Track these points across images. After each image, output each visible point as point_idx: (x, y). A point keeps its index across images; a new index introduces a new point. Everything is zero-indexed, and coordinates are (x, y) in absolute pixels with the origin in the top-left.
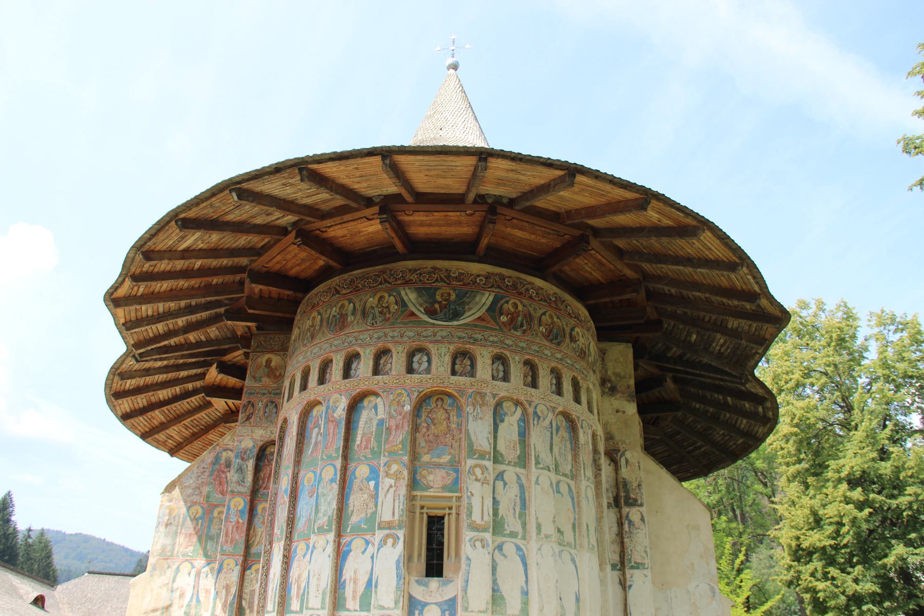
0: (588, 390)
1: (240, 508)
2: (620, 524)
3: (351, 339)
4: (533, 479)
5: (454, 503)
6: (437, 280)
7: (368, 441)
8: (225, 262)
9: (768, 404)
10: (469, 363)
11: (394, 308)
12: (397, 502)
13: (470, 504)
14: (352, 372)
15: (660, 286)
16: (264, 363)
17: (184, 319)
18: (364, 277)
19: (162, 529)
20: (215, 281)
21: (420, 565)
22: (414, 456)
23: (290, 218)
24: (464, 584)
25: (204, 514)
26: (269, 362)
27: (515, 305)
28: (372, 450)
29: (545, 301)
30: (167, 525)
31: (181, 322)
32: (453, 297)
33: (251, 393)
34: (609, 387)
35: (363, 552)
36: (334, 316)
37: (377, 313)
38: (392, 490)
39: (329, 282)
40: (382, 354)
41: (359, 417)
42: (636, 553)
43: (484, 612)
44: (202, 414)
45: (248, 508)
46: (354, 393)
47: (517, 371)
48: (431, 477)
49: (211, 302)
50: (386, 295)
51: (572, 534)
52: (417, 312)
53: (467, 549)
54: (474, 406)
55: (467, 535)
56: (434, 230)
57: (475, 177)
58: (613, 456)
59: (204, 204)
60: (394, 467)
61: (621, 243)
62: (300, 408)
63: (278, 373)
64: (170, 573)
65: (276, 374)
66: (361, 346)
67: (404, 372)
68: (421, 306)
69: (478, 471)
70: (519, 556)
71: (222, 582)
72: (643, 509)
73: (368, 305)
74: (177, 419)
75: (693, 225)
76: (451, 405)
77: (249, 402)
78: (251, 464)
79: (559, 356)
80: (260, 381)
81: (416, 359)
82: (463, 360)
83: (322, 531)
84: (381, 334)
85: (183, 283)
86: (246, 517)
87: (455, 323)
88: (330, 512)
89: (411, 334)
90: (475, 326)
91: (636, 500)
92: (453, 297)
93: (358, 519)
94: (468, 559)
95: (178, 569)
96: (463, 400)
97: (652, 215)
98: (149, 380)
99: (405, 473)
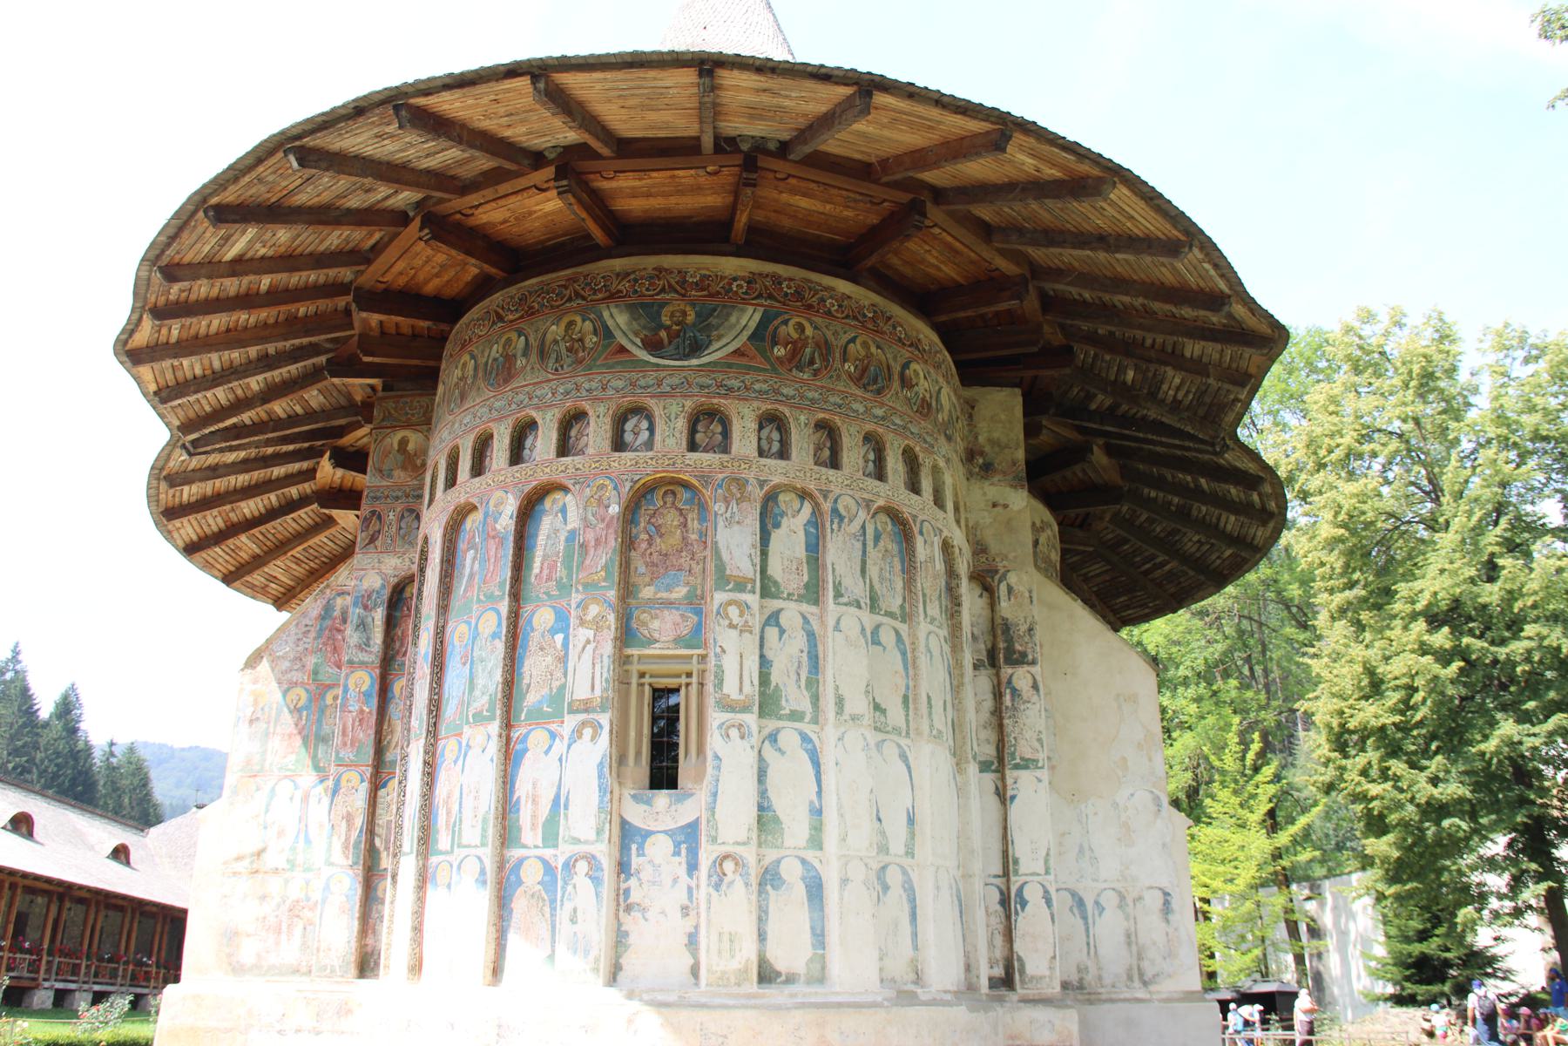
0: (936, 470)
1: (364, 688)
2: (998, 695)
3: (521, 397)
4: (831, 623)
5: (694, 667)
6: (663, 290)
7: (553, 567)
8: (312, 276)
9: (1267, 489)
10: (719, 429)
11: (591, 340)
12: (598, 667)
13: (720, 667)
14: (526, 452)
15: (1060, 287)
16: (396, 446)
17: (260, 378)
18: (541, 291)
20: (302, 311)
21: (640, 769)
22: (627, 590)
23: (405, 197)
24: (710, 800)
25: (310, 700)
26: (403, 443)
27: (800, 328)
28: (559, 582)
29: (855, 318)
30: (251, 722)
31: (255, 383)
32: (691, 318)
33: (376, 498)
34: (978, 463)
35: (547, 752)
36: (495, 360)
37: (564, 351)
38: (590, 648)
39: (486, 302)
40: (572, 421)
41: (537, 529)
42: (1023, 742)
43: (744, 844)
44: (321, 538)
45: (377, 687)
46: (528, 488)
47: (802, 441)
48: (656, 624)
49: (301, 348)
50: (578, 319)
51: (902, 713)
52: (629, 346)
53: (714, 741)
54: (727, 502)
55: (715, 718)
56: (656, 203)
57: (710, 108)
58: (986, 579)
59: (247, 179)
60: (594, 610)
61: (984, 212)
62: (444, 518)
63: (419, 462)
65: (414, 463)
66: (538, 408)
67: (608, 449)
68: (636, 334)
69: (733, 612)
70: (806, 750)
71: (341, 810)
72: (1036, 670)
73: (549, 337)
74: (280, 548)
75: (1094, 175)
76: (689, 501)
77: (373, 513)
78: (379, 615)
79: (879, 412)
80: (390, 476)
81: (629, 426)
82: (707, 426)
83: (479, 719)
84: (570, 386)
85: (243, 317)
86: (374, 702)
87: (694, 362)
88: (492, 689)
89: (620, 384)
90: (730, 366)
91: (1024, 654)
92: (691, 318)
93: (538, 697)
94: (717, 757)
95: (273, 790)
96: (707, 493)
97: (1021, 160)
98: (221, 484)
99: (612, 618)
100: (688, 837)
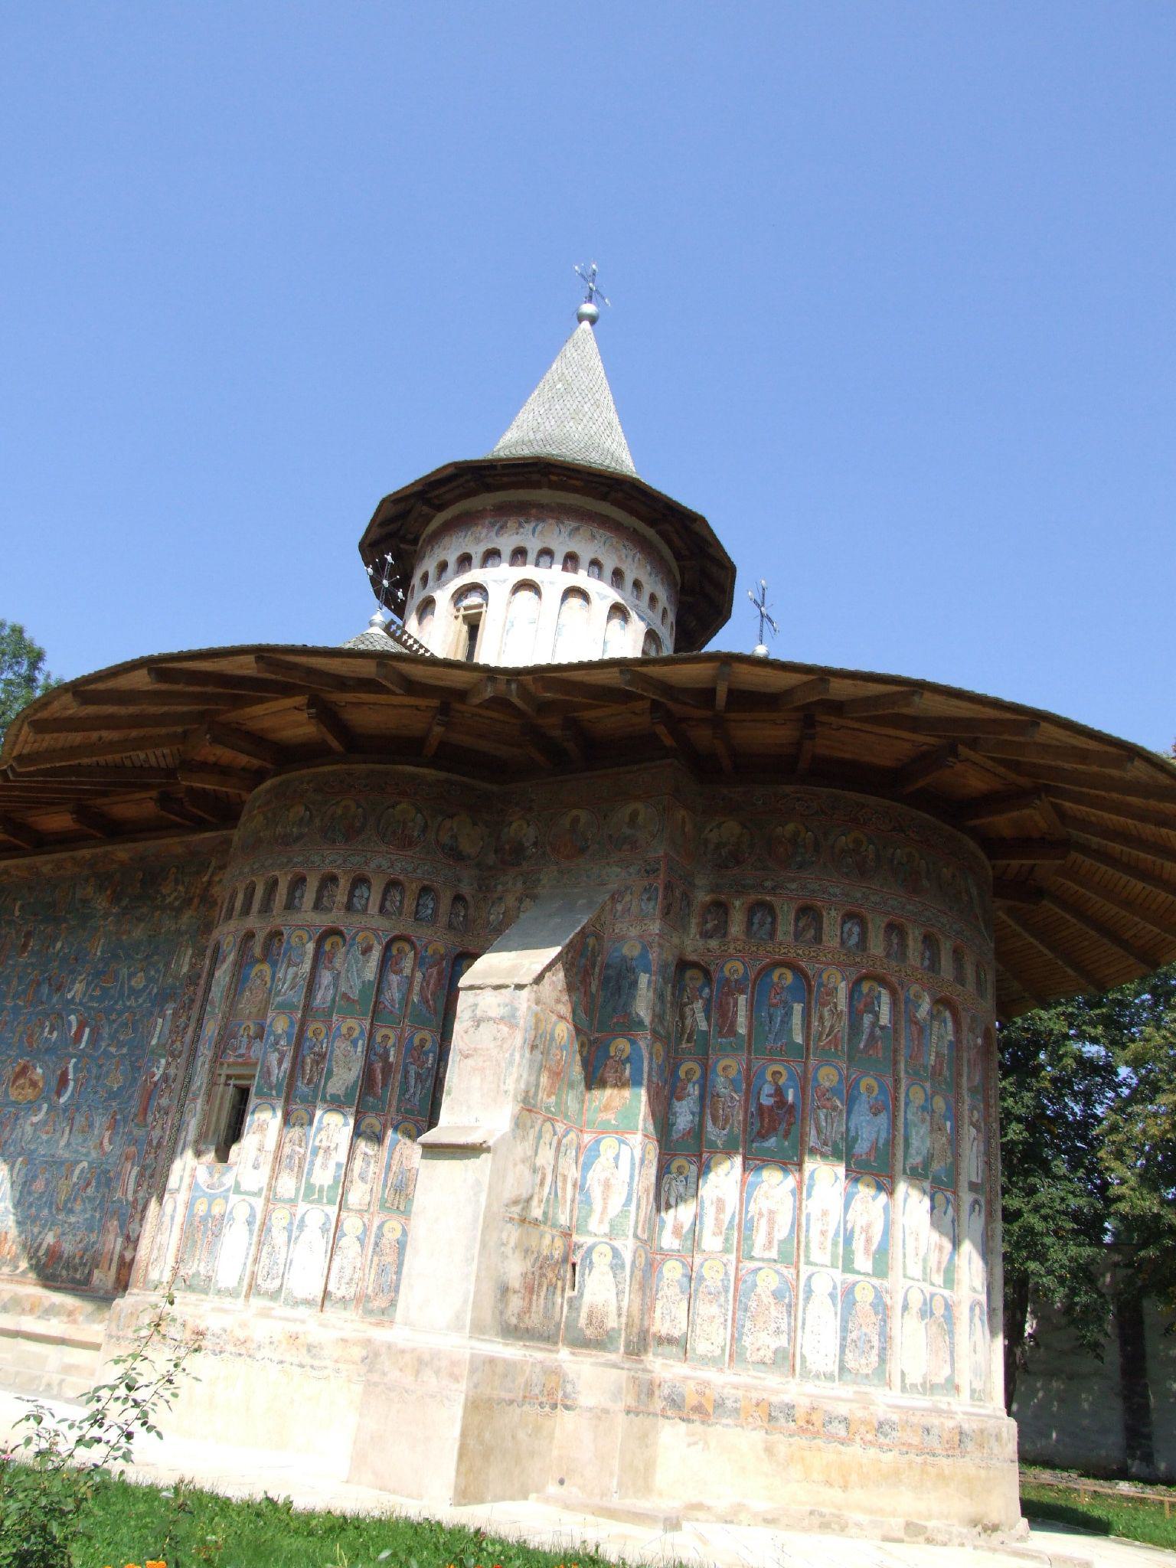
64: (532, 1134)
95: (540, 1131)
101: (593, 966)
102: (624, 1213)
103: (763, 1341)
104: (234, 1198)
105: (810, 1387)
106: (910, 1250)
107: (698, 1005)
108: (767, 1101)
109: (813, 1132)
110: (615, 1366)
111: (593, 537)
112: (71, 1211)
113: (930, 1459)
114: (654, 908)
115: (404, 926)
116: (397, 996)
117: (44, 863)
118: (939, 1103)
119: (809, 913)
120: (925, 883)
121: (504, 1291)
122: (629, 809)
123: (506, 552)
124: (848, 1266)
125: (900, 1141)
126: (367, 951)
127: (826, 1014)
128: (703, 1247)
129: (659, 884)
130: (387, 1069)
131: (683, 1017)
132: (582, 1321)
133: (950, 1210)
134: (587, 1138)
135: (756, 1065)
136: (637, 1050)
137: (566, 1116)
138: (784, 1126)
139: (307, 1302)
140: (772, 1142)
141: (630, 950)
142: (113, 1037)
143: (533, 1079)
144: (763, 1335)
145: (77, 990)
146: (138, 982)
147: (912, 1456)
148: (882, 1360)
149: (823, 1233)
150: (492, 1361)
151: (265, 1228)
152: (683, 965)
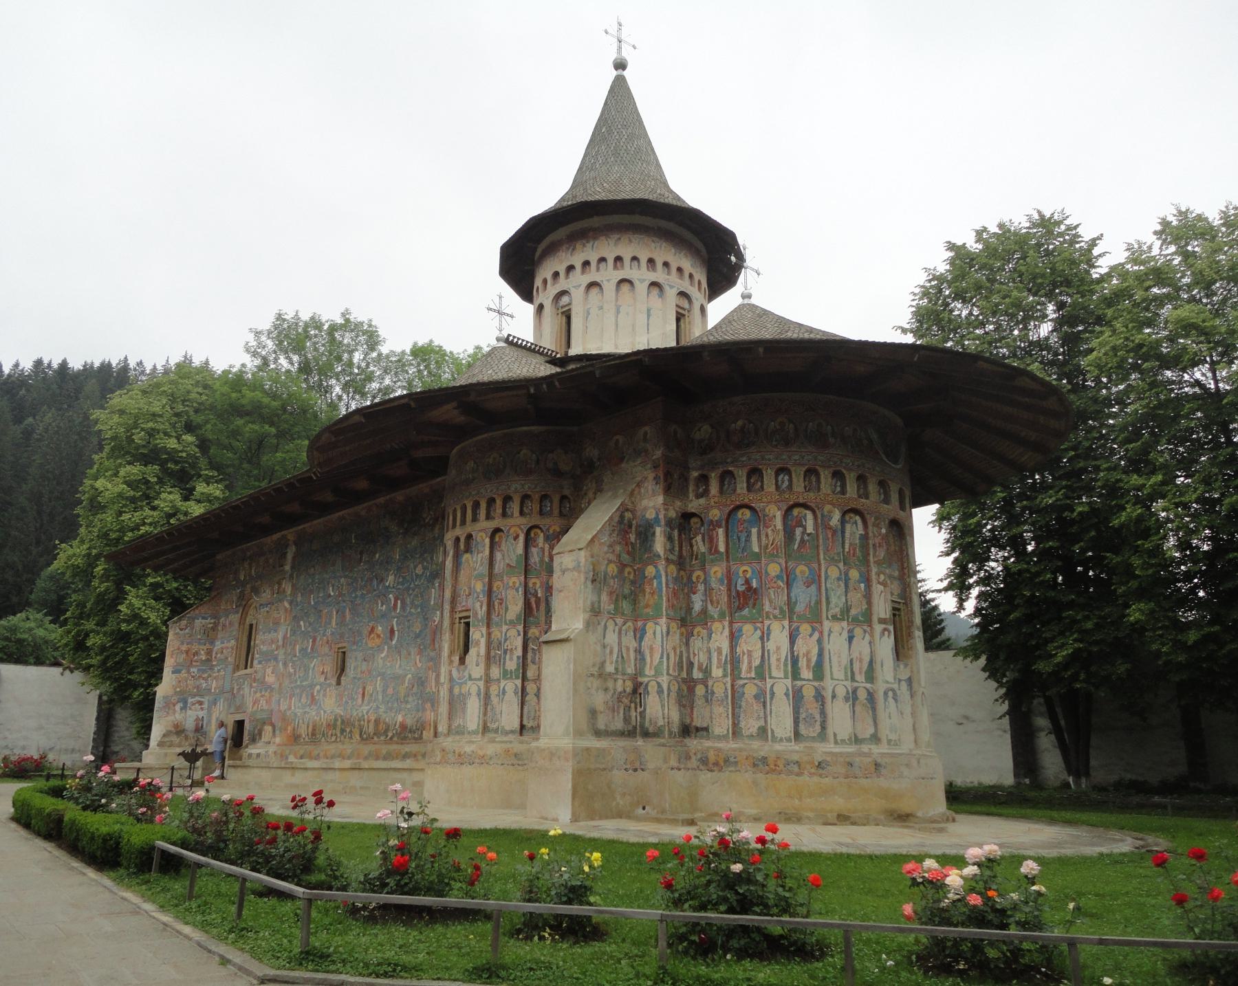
7: (854, 550)
11: (865, 442)
19: (589, 583)
64: (600, 629)
78: (676, 533)
83: (835, 618)
100: (910, 681)
101: (630, 527)
102: (661, 662)
103: (750, 725)
104: (470, 683)
105: (778, 747)
106: (835, 663)
107: (699, 538)
108: (741, 588)
109: (767, 603)
110: (664, 745)
111: (630, 241)
112: (407, 702)
113: (854, 780)
114: (659, 489)
115: (536, 520)
116: (537, 560)
117: (361, 509)
118: (854, 574)
119: (755, 473)
120: (831, 440)
121: (593, 713)
122: (641, 432)
123: (578, 266)
124: (796, 675)
125: (824, 599)
126: (516, 538)
127: (770, 532)
128: (714, 675)
129: (661, 475)
130: (538, 601)
131: (691, 546)
132: (647, 724)
133: (867, 637)
134: (640, 624)
135: (733, 568)
136: (658, 571)
137: (623, 614)
138: (751, 603)
139: (512, 732)
140: (746, 612)
141: (650, 515)
142: (412, 603)
143: (595, 599)
144: (751, 721)
145: (391, 578)
146: (419, 570)
147: (842, 780)
148: (823, 728)
149: (778, 660)
150: (588, 749)
151: (487, 696)
152: (687, 516)
